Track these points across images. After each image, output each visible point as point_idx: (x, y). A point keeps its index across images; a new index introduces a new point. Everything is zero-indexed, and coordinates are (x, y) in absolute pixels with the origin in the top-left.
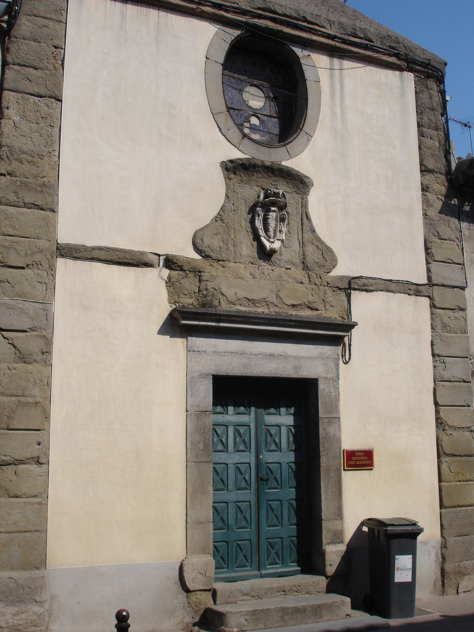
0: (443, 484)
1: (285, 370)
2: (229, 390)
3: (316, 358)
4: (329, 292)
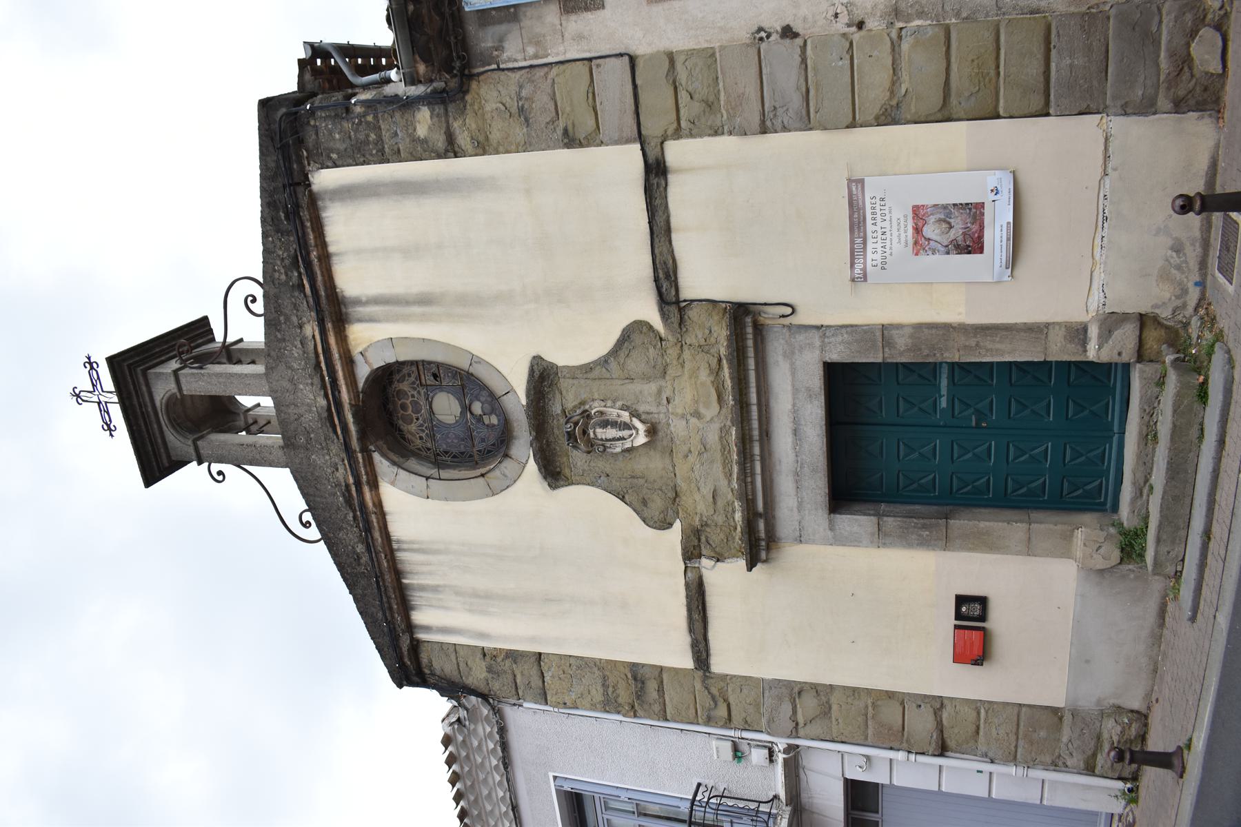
0: (1001, 113)
1: (814, 413)
2: (848, 489)
3: (792, 364)
4: (689, 339)
